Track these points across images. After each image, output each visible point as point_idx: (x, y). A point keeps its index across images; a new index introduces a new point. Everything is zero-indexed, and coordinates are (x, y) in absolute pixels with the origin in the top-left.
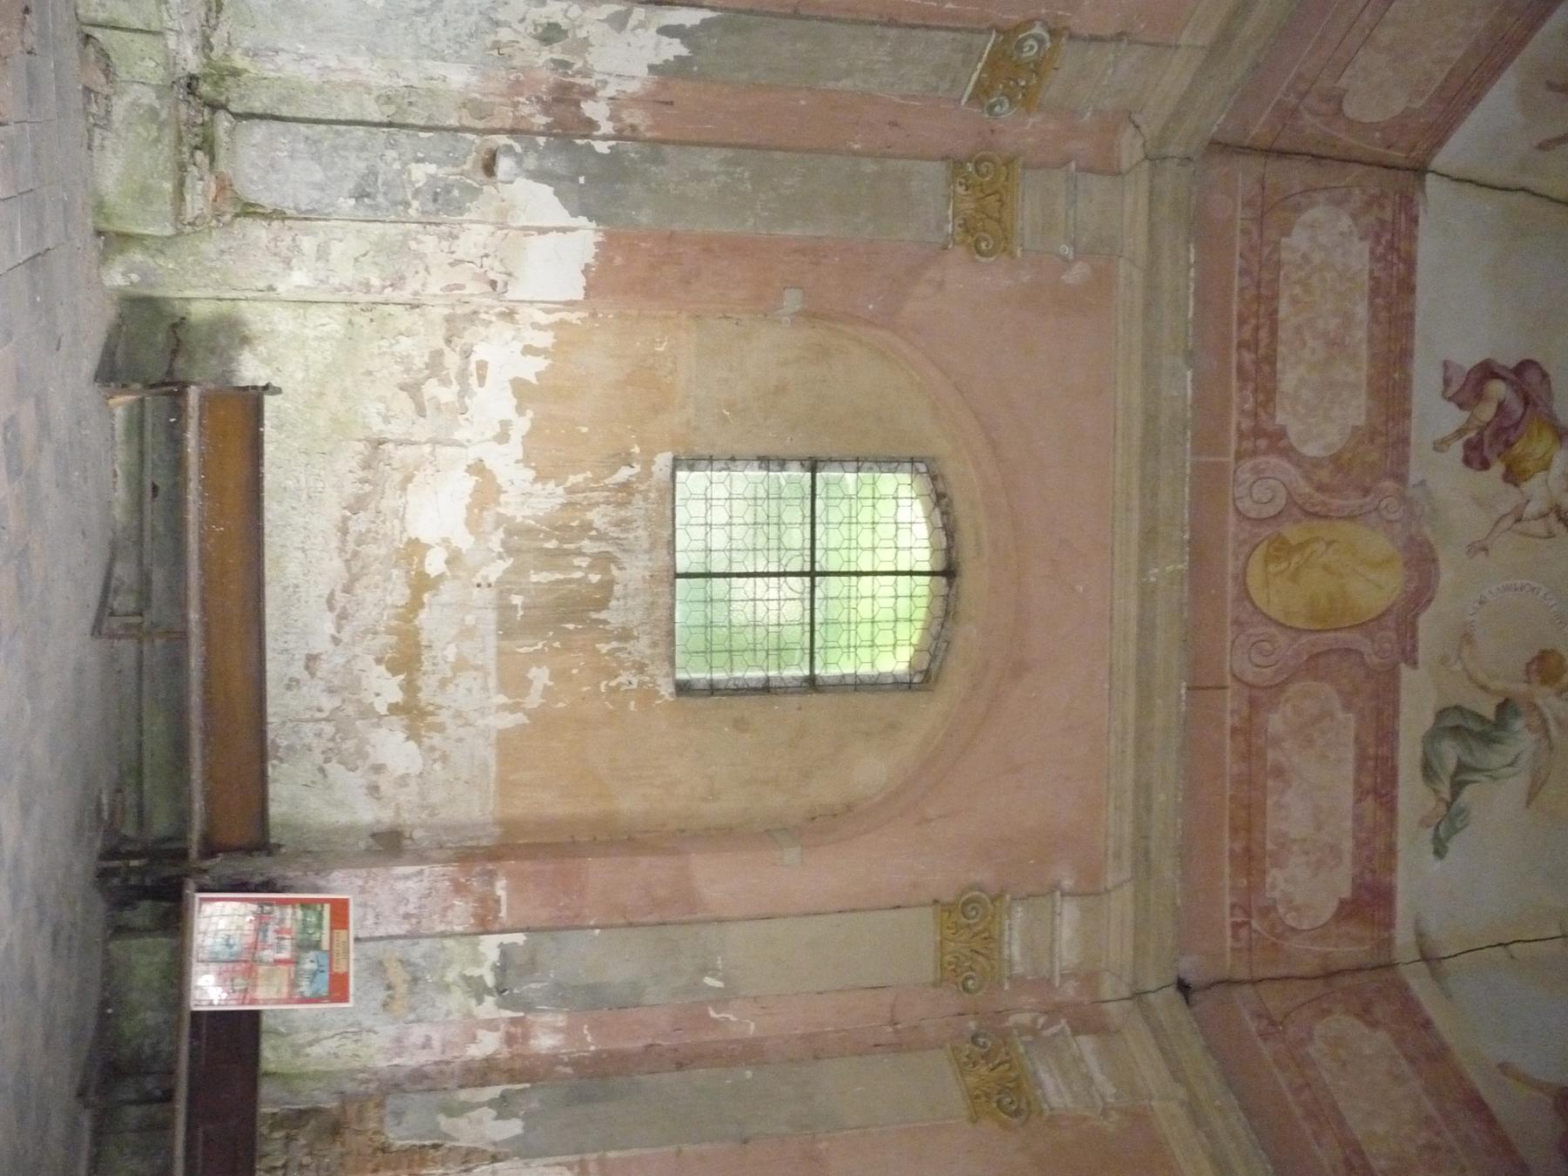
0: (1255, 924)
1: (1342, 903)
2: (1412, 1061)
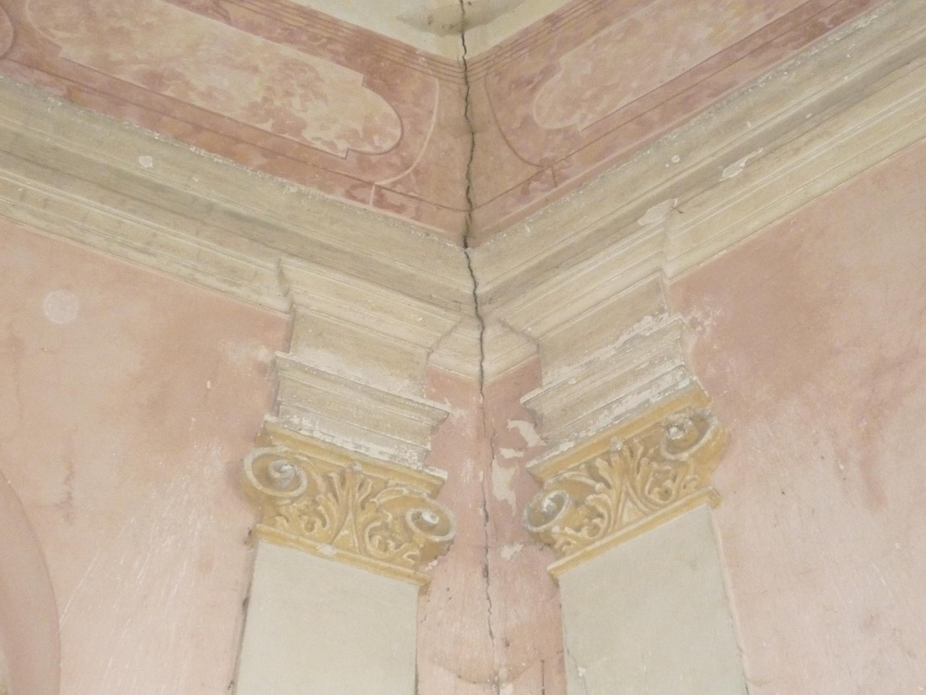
0: (383, 183)
1: (370, 84)
2: (605, 24)
